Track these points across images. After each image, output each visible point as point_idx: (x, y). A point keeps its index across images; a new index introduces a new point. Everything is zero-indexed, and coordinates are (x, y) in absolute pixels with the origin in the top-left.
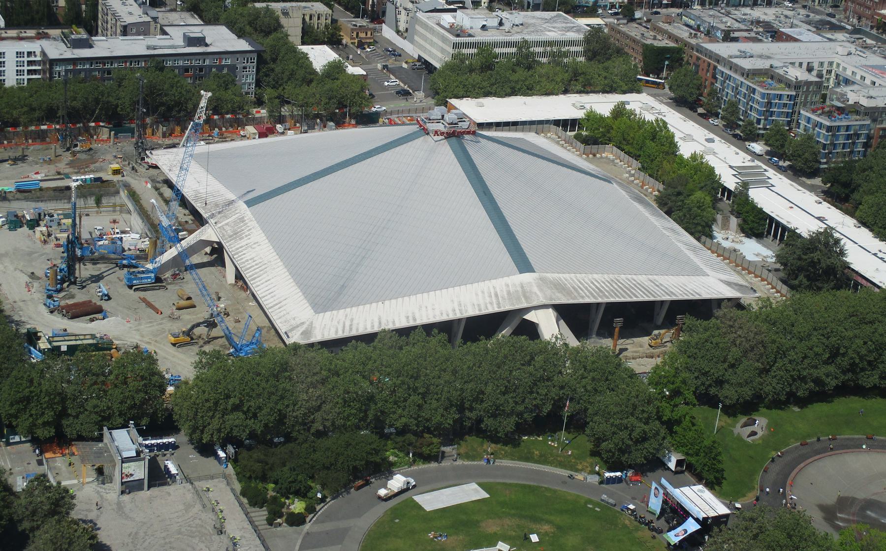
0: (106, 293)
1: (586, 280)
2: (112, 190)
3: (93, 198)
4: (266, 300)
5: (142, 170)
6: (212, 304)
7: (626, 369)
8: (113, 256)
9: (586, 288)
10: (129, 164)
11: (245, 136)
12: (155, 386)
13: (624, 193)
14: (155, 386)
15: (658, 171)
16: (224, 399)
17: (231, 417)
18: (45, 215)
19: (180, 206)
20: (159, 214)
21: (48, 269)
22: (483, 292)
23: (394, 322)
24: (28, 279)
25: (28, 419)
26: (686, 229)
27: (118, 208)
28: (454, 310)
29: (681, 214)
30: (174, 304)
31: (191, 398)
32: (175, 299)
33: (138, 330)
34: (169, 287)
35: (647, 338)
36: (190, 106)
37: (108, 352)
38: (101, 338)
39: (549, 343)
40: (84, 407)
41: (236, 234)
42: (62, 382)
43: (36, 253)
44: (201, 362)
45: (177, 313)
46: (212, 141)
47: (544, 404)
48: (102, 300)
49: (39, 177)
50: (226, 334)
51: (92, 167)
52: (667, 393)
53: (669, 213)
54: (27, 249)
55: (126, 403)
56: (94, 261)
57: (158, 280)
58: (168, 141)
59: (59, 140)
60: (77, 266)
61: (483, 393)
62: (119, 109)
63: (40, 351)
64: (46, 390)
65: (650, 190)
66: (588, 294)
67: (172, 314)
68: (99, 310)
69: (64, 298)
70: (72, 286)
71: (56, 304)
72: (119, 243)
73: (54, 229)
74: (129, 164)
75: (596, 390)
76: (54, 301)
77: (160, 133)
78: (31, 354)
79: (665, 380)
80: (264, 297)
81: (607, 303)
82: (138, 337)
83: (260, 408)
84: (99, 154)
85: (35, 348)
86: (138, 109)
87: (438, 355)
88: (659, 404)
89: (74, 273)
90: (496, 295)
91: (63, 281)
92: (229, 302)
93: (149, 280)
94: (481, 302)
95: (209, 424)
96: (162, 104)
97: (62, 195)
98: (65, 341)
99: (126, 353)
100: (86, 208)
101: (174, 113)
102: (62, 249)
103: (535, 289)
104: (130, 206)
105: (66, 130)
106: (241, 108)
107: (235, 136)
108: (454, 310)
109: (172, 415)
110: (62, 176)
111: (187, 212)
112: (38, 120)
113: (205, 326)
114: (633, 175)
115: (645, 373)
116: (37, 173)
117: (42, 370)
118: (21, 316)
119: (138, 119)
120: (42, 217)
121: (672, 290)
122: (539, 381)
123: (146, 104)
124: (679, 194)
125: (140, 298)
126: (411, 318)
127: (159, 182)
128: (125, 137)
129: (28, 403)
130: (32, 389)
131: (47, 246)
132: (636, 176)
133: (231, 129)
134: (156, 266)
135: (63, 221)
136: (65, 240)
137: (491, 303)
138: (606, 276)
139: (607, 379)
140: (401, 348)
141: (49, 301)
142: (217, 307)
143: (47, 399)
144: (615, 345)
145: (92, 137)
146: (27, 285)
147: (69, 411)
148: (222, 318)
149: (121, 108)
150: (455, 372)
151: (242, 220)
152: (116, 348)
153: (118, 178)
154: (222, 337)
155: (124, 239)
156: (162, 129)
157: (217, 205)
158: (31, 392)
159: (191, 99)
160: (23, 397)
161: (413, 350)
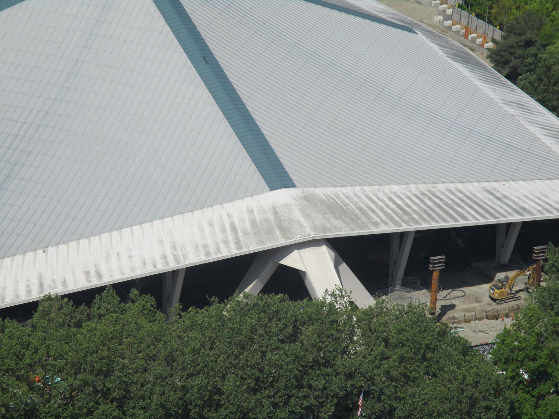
1: (380, 195)
7: (457, 340)
9: (381, 209)
13: (436, 47)
15: (491, 8)
22: (211, 225)
23: (64, 283)
26: (543, 102)
28: (164, 257)
29: (533, 77)
35: (485, 287)
39: (323, 304)
47: (322, 405)
52: (526, 376)
53: (512, 77)
61: (219, 391)
65: (480, 40)
66: (384, 218)
75: (407, 377)
79: (521, 355)
81: (417, 232)
87: (142, 332)
88: (514, 396)
90: (234, 228)
94: (210, 241)
103: (297, 215)
108: (164, 257)
114: (450, 17)
115: (487, 344)
121: (523, 204)
122: (311, 367)
124: (529, 44)
126: (93, 274)
132: (456, 17)
137: (226, 242)
138: (413, 187)
139: (424, 359)
140: (78, 325)
144: (434, 301)
150: (170, 360)
161: (99, 327)
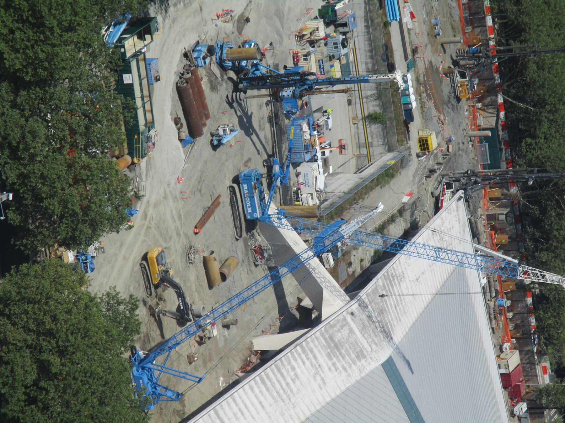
0: (224, 141)
2: (394, 139)
3: (378, 110)
4: (229, 405)
5: (431, 184)
6: (216, 315)
8: (285, 148)
10: (439, 164)
11: (502, 351)
12: (74, 230)
14: (74, 230)
16: (58, 346)
17: (28, 361)
18: (344, 34)
19: (376, 252)
20: (360, 218)
21: (256, 44)
24: (237, 12)
25: (5, 26)
27: (364, 151)
30: (212, 252)
31: (57, 290)
32: (221, 253)
33: (165, 198)
34: (241, 243)
36: (544, 256)
37: (126, 151)
38: (149, 138)
40: (31, 116)
41: (336, 346)
42: (71, 79)
43: (282, 23)
44: (119, 303)
45: (198, 259)
46: (488, 297)
48: (212, 135)
49: (406, 19)
50: (167, 341)
51: (430, 104)
54: (286, 9)
55: (43, 184)
56: (274, 119)
57: (251, 224)
58: (482, 225)
59: (469, 46)
60: (264, 92)
62: (529, 140)
63: (121, 40)
64: (57, 55)
67: (196, 251)
68: (194, 132)
69: (211, 74)
70: (231, 85)
71: (200, 62)
72: (308, 157)
73: (323, 50)
74: (439, 164)
76: (204, 58)
77: (494, 210)
78: (115, 25)
80: (234, 401)
82: (153, 200)
83: (45, 408)
84: (452, 114)
85: (125, 32)
86: (532, 172)
89: (252, 87)
91: (238, 70)
92: (221, 344)
93: (250, 210)
95: (14, 324)
96: (543, 211)
97: (379, 58)
98: (140, 80)
99: (126, 180)
100: (361, 98)
101: (530, 230)
102: (290, 64)
104: (370, 171)
105: (488, 57)
106: (549, 341)
107: (500, 334)
109: (27, 262)
110: (410, 57)
111: (367, 264)
112: (500, 11)
113: (179, 306)
116: (412, 16)
117: (90, 46)
118: (175, 5)
119: (515, 172)
120: (341, 29)
123: (540, 184)
125: (219, 196)
127: (412, 214)
128: (483, 155)
129: (33, 25)
130: (57, 30)
131: (294, 41)
133: (511, 327)
134: (274, 219)
135: (337, 64)
136: (305, 69)
141: (205, 50)
142: (213, 324)
143: (42, 56)
145: (479, 100)
146: (228, 12)
147: (23, 93)
148: (194, 333)
149: (531, 144)
151: (360, 355)
152: (133, 163)
153: (415, 148)
154: (162, 335)
155: (314, 165)
156: (502, 213)
157: (381, 312)
158: (51, 29)
159: (556, 257)
160: (42, 17)
